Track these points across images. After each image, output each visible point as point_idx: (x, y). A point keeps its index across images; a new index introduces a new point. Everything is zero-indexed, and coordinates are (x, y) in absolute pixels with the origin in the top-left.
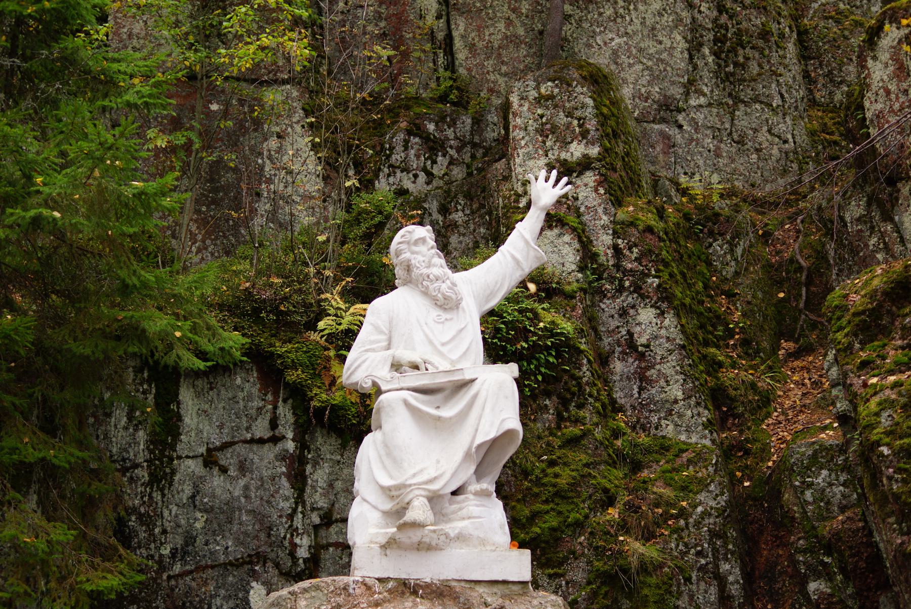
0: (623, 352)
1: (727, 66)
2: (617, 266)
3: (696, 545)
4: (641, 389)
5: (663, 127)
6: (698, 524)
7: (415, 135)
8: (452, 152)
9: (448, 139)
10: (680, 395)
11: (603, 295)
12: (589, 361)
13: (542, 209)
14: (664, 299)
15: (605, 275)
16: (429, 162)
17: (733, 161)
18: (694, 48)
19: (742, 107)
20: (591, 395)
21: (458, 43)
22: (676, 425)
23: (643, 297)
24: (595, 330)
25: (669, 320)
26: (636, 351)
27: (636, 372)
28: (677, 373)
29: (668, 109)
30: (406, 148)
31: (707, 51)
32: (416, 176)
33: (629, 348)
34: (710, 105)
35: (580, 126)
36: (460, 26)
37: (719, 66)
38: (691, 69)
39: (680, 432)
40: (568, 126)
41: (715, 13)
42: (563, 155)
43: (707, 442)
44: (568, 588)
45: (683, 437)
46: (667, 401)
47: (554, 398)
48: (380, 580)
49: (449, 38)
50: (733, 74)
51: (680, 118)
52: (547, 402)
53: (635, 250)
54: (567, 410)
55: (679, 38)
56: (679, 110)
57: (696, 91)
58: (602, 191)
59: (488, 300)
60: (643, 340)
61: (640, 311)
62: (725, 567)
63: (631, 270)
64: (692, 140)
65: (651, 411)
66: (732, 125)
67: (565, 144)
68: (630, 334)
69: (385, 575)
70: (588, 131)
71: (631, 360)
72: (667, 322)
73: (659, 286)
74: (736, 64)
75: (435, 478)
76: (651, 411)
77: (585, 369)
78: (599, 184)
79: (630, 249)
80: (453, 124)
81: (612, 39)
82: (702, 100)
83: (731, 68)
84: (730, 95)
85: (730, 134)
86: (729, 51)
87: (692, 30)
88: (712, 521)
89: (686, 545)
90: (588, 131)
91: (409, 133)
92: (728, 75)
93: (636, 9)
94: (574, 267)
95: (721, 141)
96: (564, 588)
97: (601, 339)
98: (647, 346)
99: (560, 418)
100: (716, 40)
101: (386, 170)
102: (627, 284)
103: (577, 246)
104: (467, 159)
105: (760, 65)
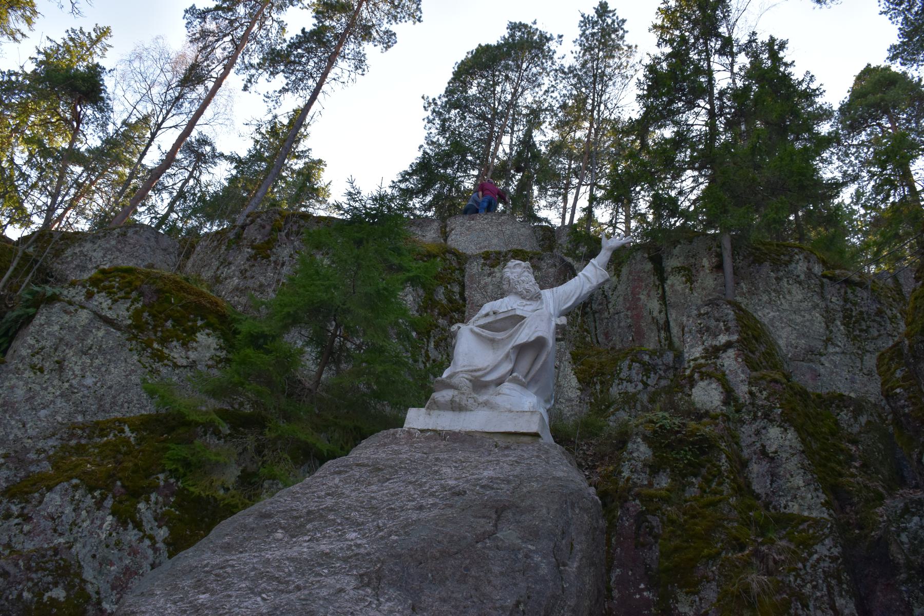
0: (759, 458)
1: (854, 331)
2: (753, 404)
3: (812, 581)
4: (772, 482)
5: (811, 364)
6: (813, 566)
7: (636, 362)
8: (661, 372)
9: (657, 365)
10: (801, 483)
11: (742, 422)
12: (727, 457)
13: (608, 249)
14: (786, 421)
15: (744, 410)
16: (645, 378)
17: (866, 386)
18: (829, 321)
19: (868, 354)
20: (727, 477)
21: (672, 324)
22: (800, 505)
23: (771, 421)
24: (737, 444)
25: (791, 434)
26: (768, 456)
27: (768, 471)
28: (798, 468)
29: (812, 354)
30: (630, 369)
31: (839, 323)
32: (636, 386)
33: (763, 454)
34: (843, 353)
35: (725, 325)
36: (673, 315)
37: (849, 331)
38: (828, 332)
39: (803, 510)
40: (717, 327)
41: (842, 303)
42: (714, 343)
43: (826, 516)
44: (701, 603)
45: (806, 514)
46: (792, 488)
47: (700, 479)
48: (422, 431)
49: (667, 322)
50: (859, 336)
51: (822, 359)
52: (694, 480)
53: (765, 393)
54: (709, 487)
55: (817, 315)
56: (821, 355)
57: (832, 344)
58: (740, 360)
59: (565, 303)
60: (773, 449)
61: (769, 430)
62: (840, 602)
63: (762, 405)
64: (833, 372)
65: (780, 496)
66: (862, 364)
67: (716, 336)
68: (764, 446)
69: (426, 428)
70: (729, 328)
71: (764, 463)
72: (789, 436)
73: (782, 412)
74: (861, 331)
75: (479, 370)
76: (780, 496)
77: (724, 461)
78: (738, 356)
79: (761, 392)
80: (661, 355)
81: (768, 313)
82: (837, 349)
83: (857, 333)
84: (859, 348)
85: (861, 370)
86: (854, 323)
87: (827, 312)
88: (826, 564)
89: (803, 580)
90: (729, 328)
91: (632, 361)
92: (855, 337)
93: (784, 297)
94: (719, 403)
95: (855, 374)
96: (698, 603)
97: (742, 451)
98: (776, 452)
99: (703, 491)
100: (845, 317)
101: (617, 381)
102: (760, 414)
103: (721, 390)
104: (671, 376)
105: (878, 331)
